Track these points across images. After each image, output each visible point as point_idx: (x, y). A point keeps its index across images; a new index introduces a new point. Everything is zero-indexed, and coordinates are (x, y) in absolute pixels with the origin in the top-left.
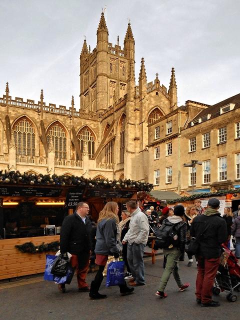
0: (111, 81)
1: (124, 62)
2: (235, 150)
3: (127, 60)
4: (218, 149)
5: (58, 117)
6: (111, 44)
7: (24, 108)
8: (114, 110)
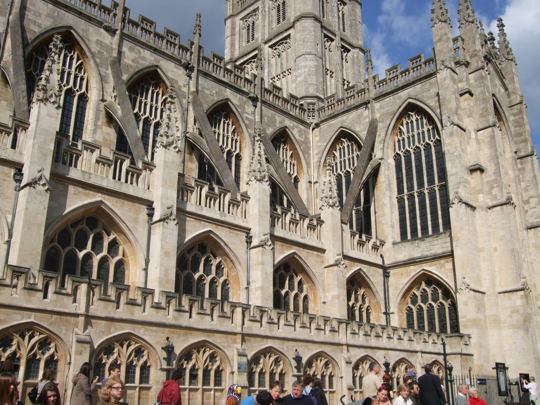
0: (326, 36)
5: (229, 93)
7: (155, 50)
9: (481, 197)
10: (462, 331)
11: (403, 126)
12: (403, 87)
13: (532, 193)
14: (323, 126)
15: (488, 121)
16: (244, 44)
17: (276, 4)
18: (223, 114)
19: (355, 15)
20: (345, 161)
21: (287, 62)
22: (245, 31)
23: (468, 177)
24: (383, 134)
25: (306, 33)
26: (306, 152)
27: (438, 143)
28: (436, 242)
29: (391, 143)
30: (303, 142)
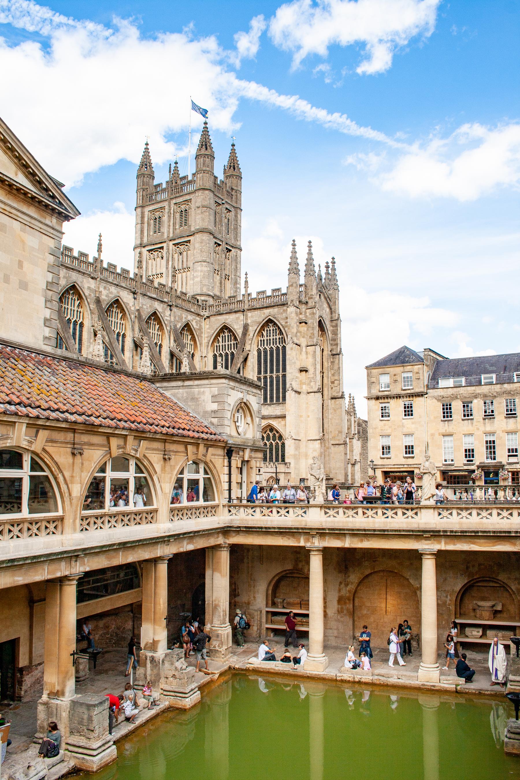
0: (216, 243)
1: (230, 211)
2: (506, 429)
3: (232, 209)
4: (485, 424)
6: (216, 178)
8: (246, 307)
9: (304, 387)
10: (287, 460)
11: (264, 330)
12: (267, 307)
13: (336, 378)
14: (213, 319)
15: (313, 342)
16: (151, 233)
17: (179, 210)
18: (153, 318)
19: (237, 221)
20: (225, 345)
21: (187, 261)
22: (152, 221)
23: (298, 374)
24: (252, 335)
25: (203, 245)
26: (200, 336)
27: (284, 348)
28: (277, 408)
29: (257, 341)
30: (198, 329)
